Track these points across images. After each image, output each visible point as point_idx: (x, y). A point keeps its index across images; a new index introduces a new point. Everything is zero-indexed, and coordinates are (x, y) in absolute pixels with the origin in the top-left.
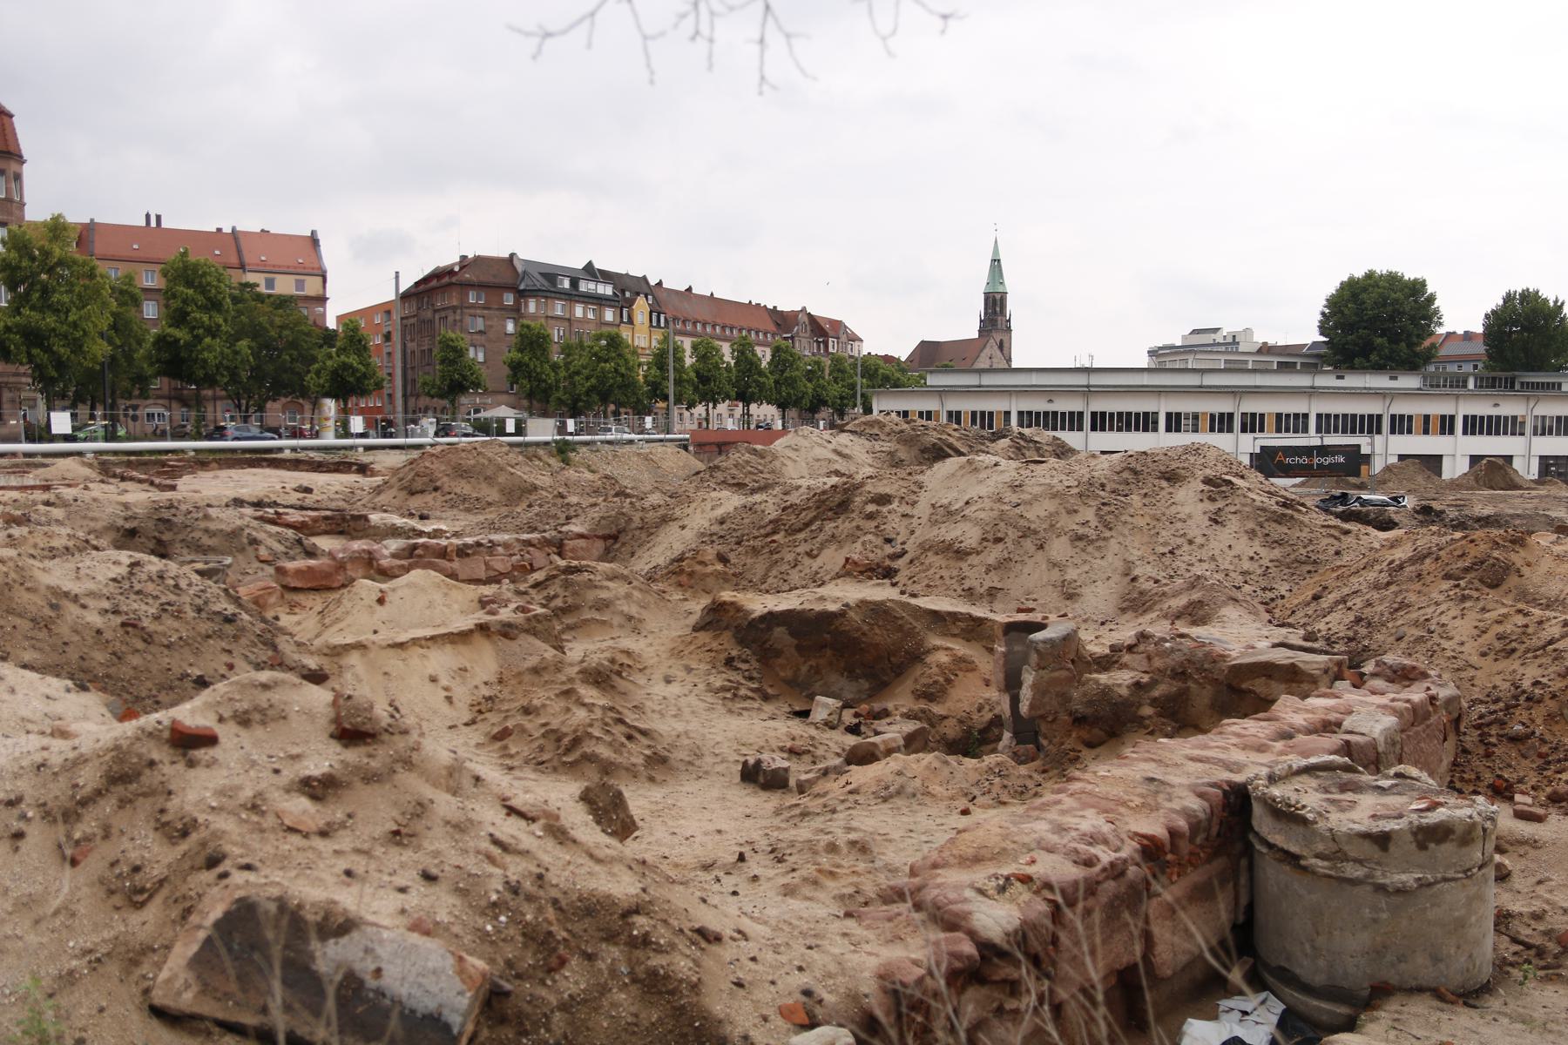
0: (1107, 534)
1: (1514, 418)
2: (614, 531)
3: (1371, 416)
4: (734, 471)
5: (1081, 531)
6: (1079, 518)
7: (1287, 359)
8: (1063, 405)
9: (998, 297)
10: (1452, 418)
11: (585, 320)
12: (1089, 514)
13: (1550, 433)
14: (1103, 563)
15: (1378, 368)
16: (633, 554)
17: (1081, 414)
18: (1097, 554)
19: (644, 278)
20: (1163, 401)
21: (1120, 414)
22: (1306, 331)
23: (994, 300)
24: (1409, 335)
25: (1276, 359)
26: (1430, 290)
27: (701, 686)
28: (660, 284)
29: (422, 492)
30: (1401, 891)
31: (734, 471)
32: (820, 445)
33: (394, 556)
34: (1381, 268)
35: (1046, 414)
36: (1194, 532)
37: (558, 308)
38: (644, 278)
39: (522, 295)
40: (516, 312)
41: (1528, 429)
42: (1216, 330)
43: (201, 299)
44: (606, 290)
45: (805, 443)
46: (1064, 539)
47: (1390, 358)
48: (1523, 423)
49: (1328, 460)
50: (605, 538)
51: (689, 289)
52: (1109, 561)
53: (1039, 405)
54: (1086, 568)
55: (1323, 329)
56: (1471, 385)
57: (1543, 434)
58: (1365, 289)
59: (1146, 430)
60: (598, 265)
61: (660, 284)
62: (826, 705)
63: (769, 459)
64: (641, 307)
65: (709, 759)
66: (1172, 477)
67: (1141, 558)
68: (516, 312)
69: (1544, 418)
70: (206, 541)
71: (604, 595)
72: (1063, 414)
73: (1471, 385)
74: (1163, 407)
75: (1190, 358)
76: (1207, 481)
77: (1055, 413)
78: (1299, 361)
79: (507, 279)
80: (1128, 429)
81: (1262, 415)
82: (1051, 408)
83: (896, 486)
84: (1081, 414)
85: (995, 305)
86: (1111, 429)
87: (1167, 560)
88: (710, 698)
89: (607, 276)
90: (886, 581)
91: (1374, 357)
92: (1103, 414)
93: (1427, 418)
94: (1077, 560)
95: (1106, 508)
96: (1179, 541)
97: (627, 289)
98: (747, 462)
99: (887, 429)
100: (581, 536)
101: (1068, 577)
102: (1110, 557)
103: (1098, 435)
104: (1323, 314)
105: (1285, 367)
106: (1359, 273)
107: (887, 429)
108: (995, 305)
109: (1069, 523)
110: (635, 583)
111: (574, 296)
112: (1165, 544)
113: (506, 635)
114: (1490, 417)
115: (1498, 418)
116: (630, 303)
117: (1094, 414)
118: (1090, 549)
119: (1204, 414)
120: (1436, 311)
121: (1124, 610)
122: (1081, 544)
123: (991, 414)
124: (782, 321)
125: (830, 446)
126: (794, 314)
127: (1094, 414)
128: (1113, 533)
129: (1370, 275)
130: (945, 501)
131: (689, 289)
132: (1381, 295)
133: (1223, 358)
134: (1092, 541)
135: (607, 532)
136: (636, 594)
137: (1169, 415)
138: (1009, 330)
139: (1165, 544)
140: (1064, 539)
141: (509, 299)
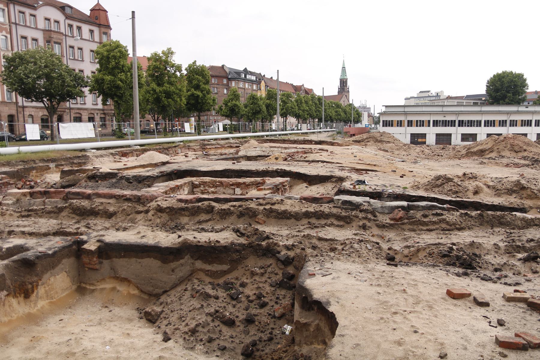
7: (476, 100)
8: (449, 118)
9: (345, 80)
10: (531, 121)
11: (248, 89)
15: (508, 104)
17: (455, 121)
19: (260, 74)
20: (483, 116)
22: (482, 90)
23: (344, 82)
24: (519, 93)
25: (472, 101)
26: (525, 77)
28: (264, 76)
34: (508, 70)
35: (443, 121)
37: (241, 85)
38: (260, 74)
39: (229, 80)
40: (228, 87)
42: (429, 91)
43: (204, 81)
44: (254, 78)
47: (512, 101)
51: (272, 78)
58: (503, 77)
60: (248, 69)
61: (264, 76)
64: (263, 84)
68: (228, 87)
72: (449, 121)
75: (446, 101)
78: (479, 102)
79: (223, 74)
81: (516, 121)
82: (444, 119)
84: (455, 121)
85: (343, 83)
89: (252, 74)
91: (507, 100)
92: (463, 121)
97: (260, 78)
103: (461, 128)
104: (487, 86)
105: (475, 104)
106: (500, 72)
108: (343, 83)
111: (245, 80)
116: (260, 82)
117: (459, 121)
120: (527, 85)
124: (297, 89)
126: (300, 87)
127: (459, 121)
129: (504, 73)
131: (272, 78)
132: (510, 79)
133: (456, 101)
138: (348, 91)
141: (225, 81)
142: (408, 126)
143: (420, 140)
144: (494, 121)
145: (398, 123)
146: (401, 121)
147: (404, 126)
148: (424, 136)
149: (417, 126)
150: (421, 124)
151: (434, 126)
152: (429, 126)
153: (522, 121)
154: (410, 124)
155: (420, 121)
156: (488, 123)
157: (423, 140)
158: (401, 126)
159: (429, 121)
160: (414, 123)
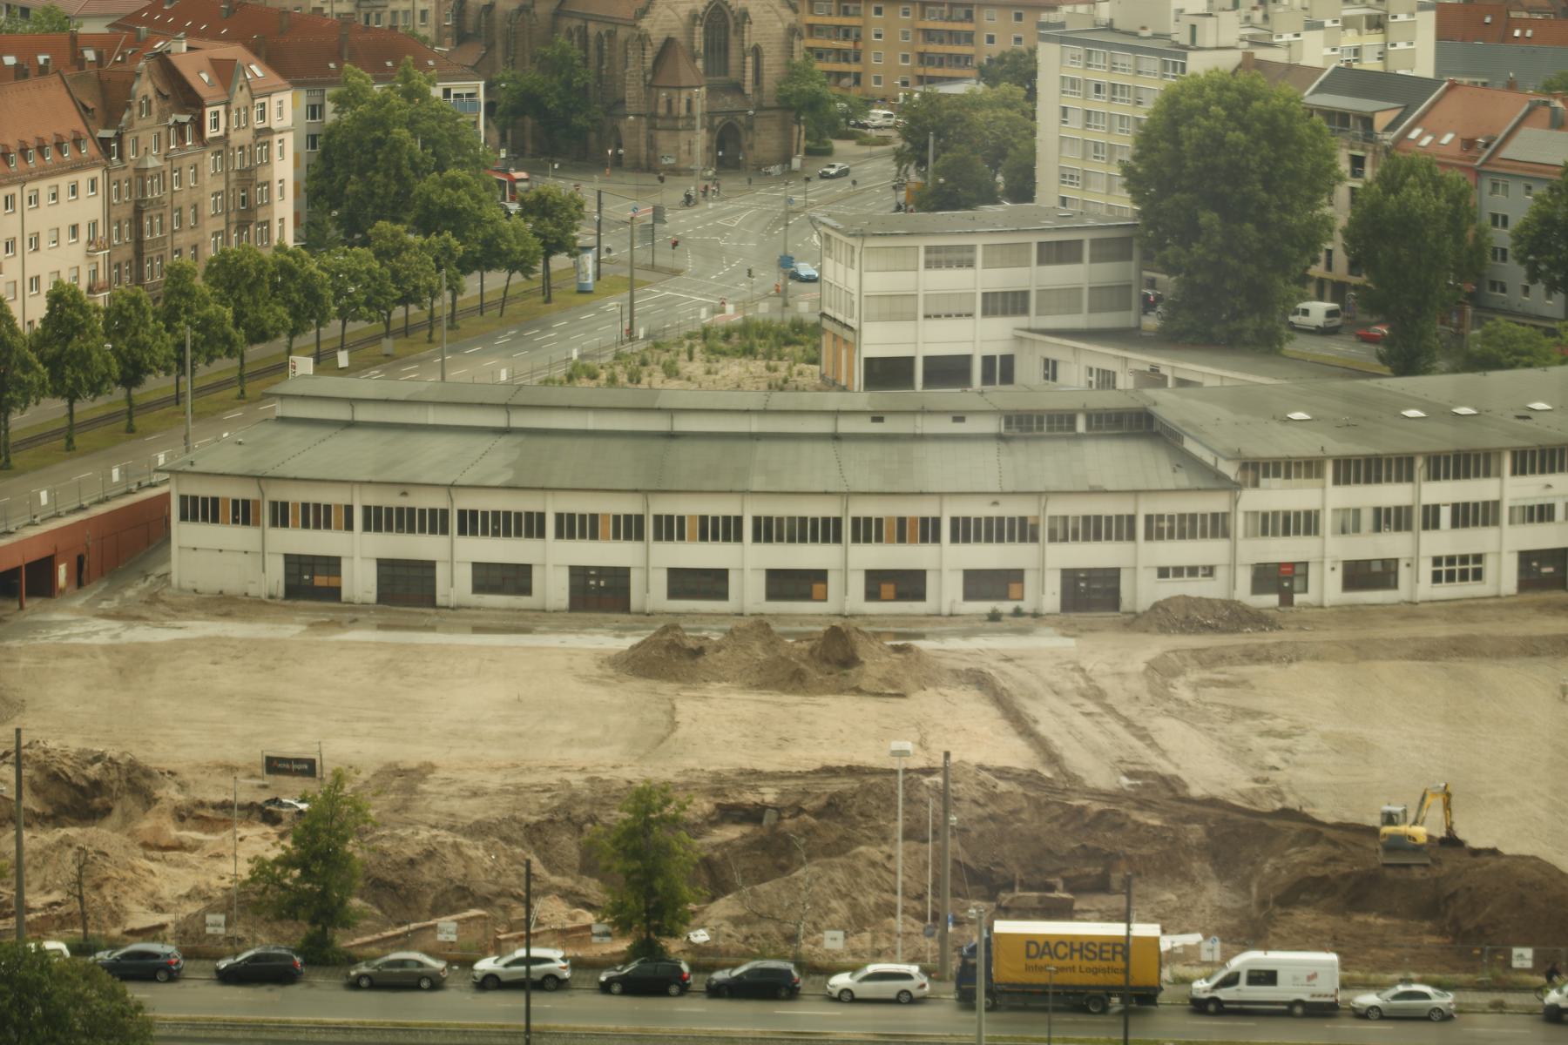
1: (1023, 520)
3: (826, 520)
13: (1075, 538)
21: (496, 514)
35: (400, 510)
41: (1044, 533)
48: (1035, 527)
49: (300, 767)
53: (391, 500)
55: (1134, 182)
56: (1081, 426)
57: (1065, 539)
58: (1190, 113)
59: (529, 535)
66: (70, 846)
69: (1065, 518)
73: (1081, 426)
74: (552, 506)
77: (411, 510)
80: (507, 534)
86: (485, 533)
92: (474, 513)
93: (902, 521)
109: (34, 862)
114: (989, 520)
115: (1000, 520)
119: (606, 516)
123: (328, 508)
127: (462, 513)
137: (559, 517)
142: (274, 524)
143: (320, 581)
144: (594, 517)
145: (235, 512)
146: (246, 503)
147: (257, 523)
148: (332, 565)
149: (306, 525)
150: (317, 517)
151: (367, 528)
152: (349, 526)
153: (703, 519)
154: (281, 515)
155: (317, 506)
156: (569, 527)
157: (333, 582)
158: (246, 522)
159: (349, 510)
160: (295, 515)
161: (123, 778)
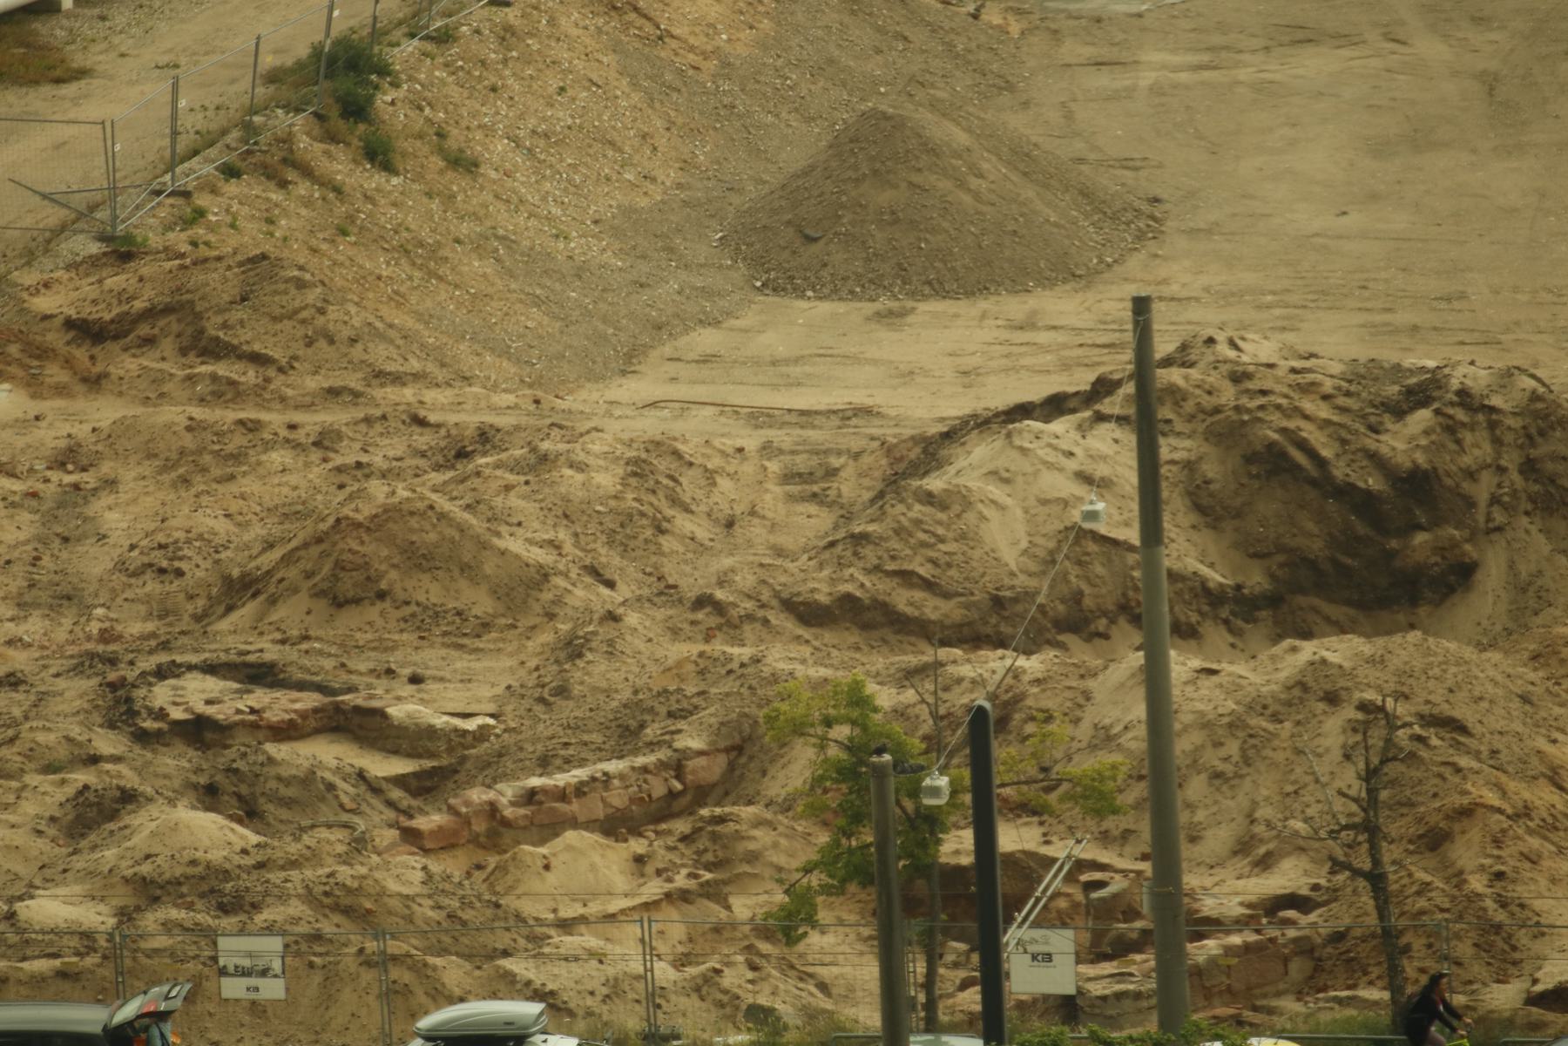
0: (1245, 770)
2: (737, 740)
4: (895, 544)
5: (1221, 766)
6: (1223, 752)
12: (1233, 748)
14: (1231, 803)
16: (764, 773)
18: (1229, 794)
27: (852, 937)
29: (357, 601)
30: (1111, 1017)
31: (895, 544)
32: (1050, 466)
33: (513, 804)
36: (1322, 769)
45: (1025, 465)
46: (1203, 776)
50: (727, 750)
52: (1234, 804)
54: (1215, 809)
62: (955, 950)
63: (957, 508)
65: (860, 994)
66: (1332, 699)
67: (1267, 799)
70: (285, 792)
71: (752, 846)
76: (1363, 707)
83: (1059, 700)
87: (1288, 801)
88: (859, 947)
90: (1035, 819)
94: (1207, 801)
95: (1252, 741)
96: (1309, 779)
98: (918, 522)
99: (1189, 407)
100: (701, 753)
101: (1196, 819)
102: (1241, 797)
107: (1189, 407)
109: (1212, 758)
110: (781, 829)
112: (1295, 782)
113: (686, 901)
118: (1224, 788)
121: (1235, 853)
122: (1217, 782)
125: (1072, 465)
128: (1250, 770)
130: (1107, 721)
134: (1227, 780)
135: (728, 743)
136: (783, 842)
139: (1295, 782)
140: (1203, 776)
161: (1511, 460)
